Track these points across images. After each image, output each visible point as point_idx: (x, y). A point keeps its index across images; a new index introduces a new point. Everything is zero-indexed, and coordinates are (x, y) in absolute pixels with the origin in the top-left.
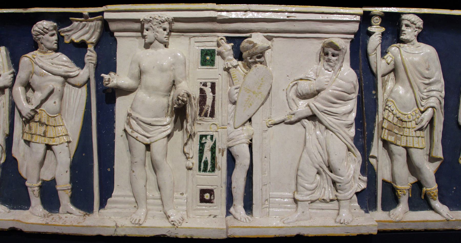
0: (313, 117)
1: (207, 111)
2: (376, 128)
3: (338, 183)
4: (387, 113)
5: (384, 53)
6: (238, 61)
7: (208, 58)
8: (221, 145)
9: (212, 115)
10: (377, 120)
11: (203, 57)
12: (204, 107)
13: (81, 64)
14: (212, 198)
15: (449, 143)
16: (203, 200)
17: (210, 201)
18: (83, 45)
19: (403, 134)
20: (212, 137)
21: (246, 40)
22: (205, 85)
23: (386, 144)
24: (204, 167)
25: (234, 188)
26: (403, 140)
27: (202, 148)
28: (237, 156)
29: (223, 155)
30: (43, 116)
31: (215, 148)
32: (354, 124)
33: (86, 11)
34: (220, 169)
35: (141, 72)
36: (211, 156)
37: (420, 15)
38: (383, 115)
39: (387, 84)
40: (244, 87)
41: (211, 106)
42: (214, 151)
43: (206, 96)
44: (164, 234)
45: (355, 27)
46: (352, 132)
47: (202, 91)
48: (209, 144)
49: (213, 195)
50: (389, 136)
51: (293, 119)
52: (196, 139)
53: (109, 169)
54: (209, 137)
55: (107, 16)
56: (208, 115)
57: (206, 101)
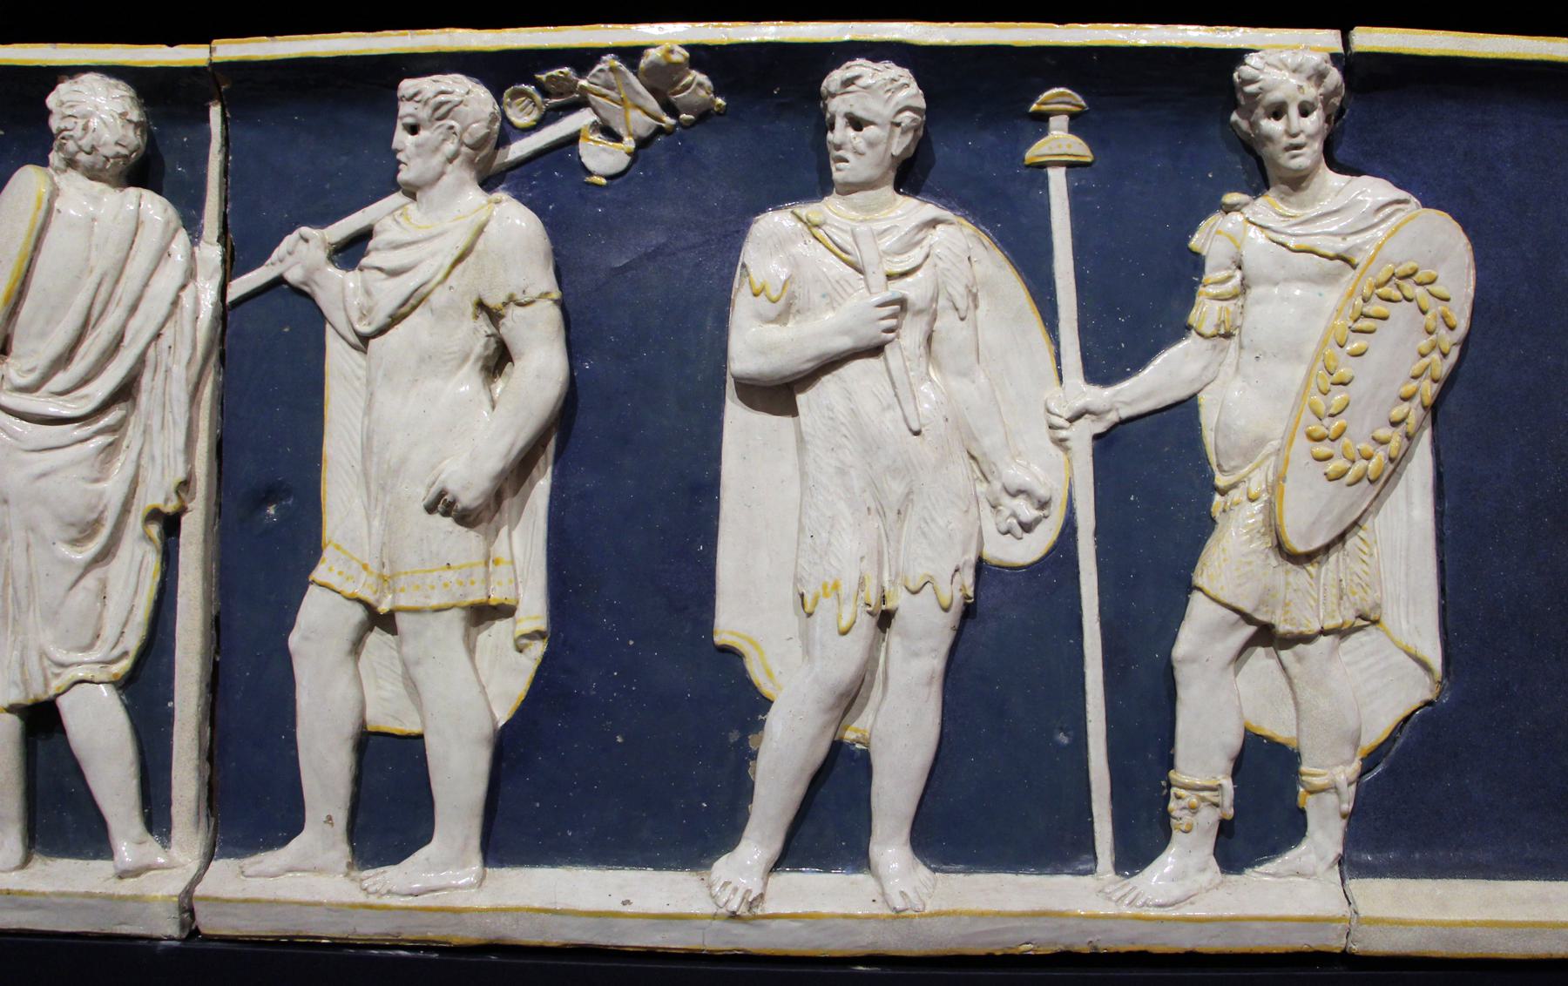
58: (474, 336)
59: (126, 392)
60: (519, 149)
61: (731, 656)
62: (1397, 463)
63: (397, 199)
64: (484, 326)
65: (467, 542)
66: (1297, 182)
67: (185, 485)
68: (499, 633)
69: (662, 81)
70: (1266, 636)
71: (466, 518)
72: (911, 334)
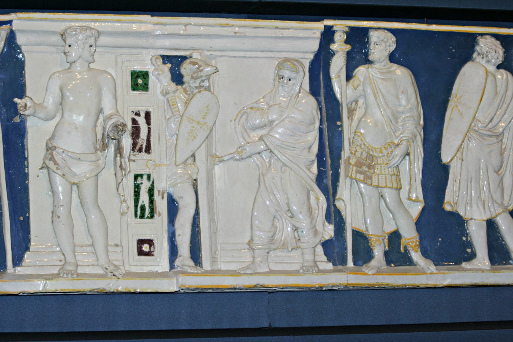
1: (142, 145)
2: (342, 166)
3: (300, 228)
4: (355, 147)
5: (349, 77)
6: (176, 84)
7: (140, 81)
9: (148, 149)
10: (343, 155)
11: (134, 80)
12: (137, 140)
14: (152, 249)
15: (431, 185)
16: (141, 253)
17: (149, 254)
19: (374, 171)
20: (149, 177)
21: (188, 61)
22: (138, 114)
24: (141, 213)
25: (179, 235)
26: (374, 179)
27: (137, 190)
28: (181, 198)
29: (163, 198)
31: (153, 189)
32: (316, 160)
34: (160, 215)
36: (149, 200)
37: (393, 31)
38: (350, 149)
39: (354, 113)
40: (187, 117)
41: (147, 140)
42: (151, 193)
43: (140, 127)
44: (104, 287)
45: (315, 46)
47: (134, 121)
49: (153, 247)
50: (358, 174)
53: (22, 217)
54: (145, 177)
56: (144, 150)
57: (140, 133)
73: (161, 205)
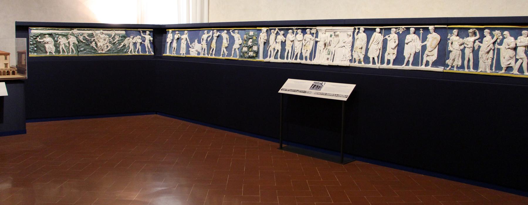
0: (344, 46)
8: (331, 51)
13: (313, 36)
16: (327, 60)
17: (328, 60)
18: (314, 33)
23: (355, 51)
30: (306, 45)
33: (314, 28)
35: (321, 38)
37: (364, 28)
45: (353, 30)
46: (351, 49)
48: (329, 50)
51: (342, 47)
52: (328, 50)
55: (317, 29)
58: (394, 41)
59: (378, 43)
60: (397, 32)
61: (404, 56)
62: (435, 48)
63: (391, 34)
64: (394, 40)
65: (393, 50)
66: (432, 33)
67: (381, 48)
68: (394, 55)
69: (403, 29)
70: (428, 56)
71: (393, 49)
72: (413, 41)
73: (331, 53)
